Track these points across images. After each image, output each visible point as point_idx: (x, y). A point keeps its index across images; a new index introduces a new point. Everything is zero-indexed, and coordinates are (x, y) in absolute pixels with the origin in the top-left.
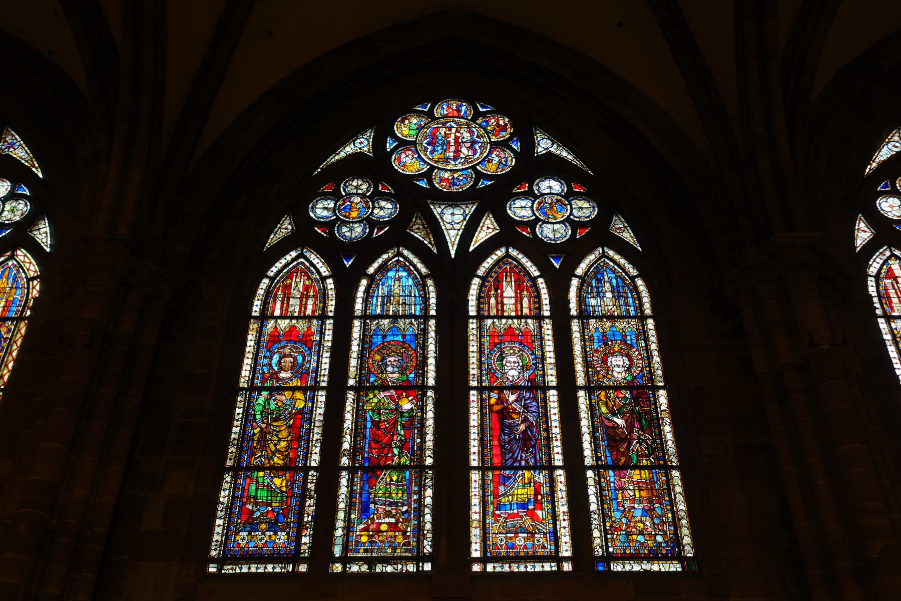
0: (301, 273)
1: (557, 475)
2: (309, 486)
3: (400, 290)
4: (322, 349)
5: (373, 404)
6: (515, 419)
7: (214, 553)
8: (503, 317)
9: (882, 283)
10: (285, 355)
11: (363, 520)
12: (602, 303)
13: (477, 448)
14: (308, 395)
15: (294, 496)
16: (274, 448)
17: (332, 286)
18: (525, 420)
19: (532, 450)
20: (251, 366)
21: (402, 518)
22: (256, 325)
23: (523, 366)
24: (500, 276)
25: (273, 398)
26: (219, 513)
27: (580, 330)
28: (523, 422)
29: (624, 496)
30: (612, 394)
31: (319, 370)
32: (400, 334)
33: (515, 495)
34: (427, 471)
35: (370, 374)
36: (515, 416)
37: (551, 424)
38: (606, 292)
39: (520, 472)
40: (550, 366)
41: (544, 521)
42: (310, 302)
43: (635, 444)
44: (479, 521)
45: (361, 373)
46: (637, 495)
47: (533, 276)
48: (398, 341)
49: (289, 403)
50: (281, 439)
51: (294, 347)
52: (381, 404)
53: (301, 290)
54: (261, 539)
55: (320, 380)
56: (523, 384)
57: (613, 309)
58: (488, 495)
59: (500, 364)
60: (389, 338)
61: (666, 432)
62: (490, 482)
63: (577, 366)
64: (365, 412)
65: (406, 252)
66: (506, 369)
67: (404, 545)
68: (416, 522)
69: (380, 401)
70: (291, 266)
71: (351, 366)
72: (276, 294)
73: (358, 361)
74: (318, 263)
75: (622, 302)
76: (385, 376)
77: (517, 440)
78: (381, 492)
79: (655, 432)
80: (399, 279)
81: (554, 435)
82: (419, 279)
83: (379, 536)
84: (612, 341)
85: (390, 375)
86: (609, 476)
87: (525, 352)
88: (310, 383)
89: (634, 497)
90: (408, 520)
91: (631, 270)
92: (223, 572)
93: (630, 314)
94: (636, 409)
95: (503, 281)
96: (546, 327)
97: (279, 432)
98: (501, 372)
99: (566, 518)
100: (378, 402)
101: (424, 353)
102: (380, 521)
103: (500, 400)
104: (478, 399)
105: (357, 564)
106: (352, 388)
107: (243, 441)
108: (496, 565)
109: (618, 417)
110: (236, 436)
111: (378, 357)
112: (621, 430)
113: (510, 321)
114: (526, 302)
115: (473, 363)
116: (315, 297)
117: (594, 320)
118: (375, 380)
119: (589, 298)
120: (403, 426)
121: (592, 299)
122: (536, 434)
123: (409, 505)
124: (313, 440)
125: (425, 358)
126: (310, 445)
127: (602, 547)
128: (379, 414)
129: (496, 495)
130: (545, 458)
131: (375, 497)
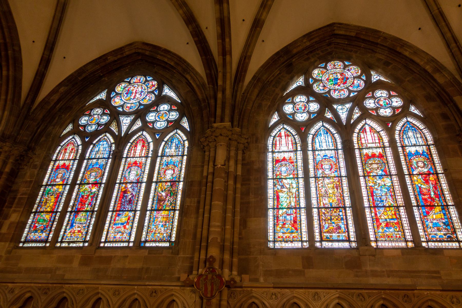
9: (275, 139)
17: (81, 148)
23: (136, 175)
28: (131, 195)
36: (128, 193)
39: (125, 212)
43: (166, 202)
48: (97, 167)
60: (95, 166)
75: (177, 150)
90: (85, 229)
91: (184, 138)
106: (78, 184)
111: (89, 173)
113: (137, 159)
114: (144, 151)
116: (74, 152)
120: (91, 197)
123: (86, 224)
125: (104, 173)
129: (115, 220)
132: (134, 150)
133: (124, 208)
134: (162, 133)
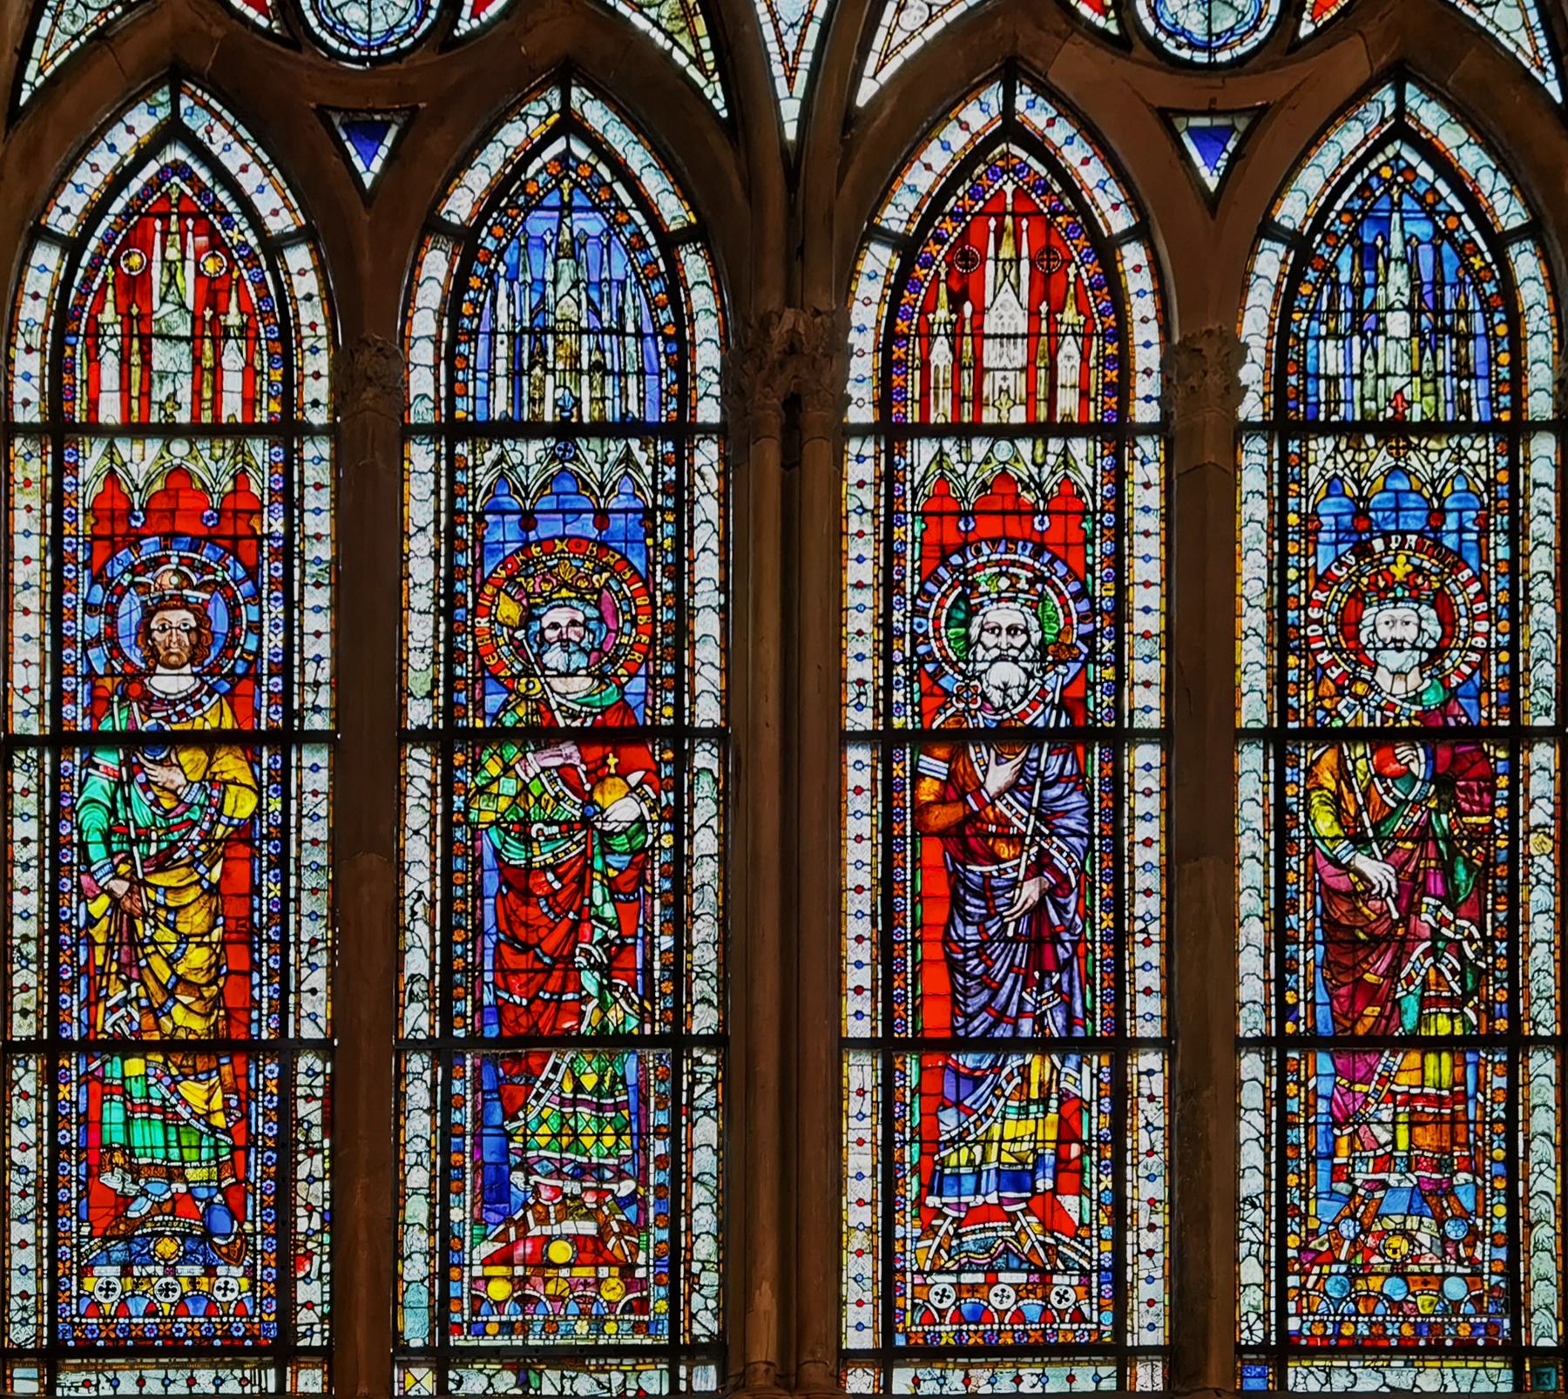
0: (182, 217)
1: (1139, 1073)
2: (303, 1109)
3: (579, 304)
4: (297, 572)
5: (503, 803)
6: (1005, 861)
7: (20, 1335)
8: (976, 429)
10: (162, 598)
11: (491, 1227)
12: (1369, 364)
13: (867, 970)
14: (265, 765)
15: (255, 1144)
16: (168, 973)
18: (1042, 864)
19: (1060, 981)
20: (42, 644)
21: (619, 1222)
22: (35, 464)
23: (1042, 646)
24: (974, 235)
25: (141, 778)
26: (15, 1201)
27: (1270, 488)
28: (1035, 870)
29: (1357, 1145)
30: (1361, 764)
31: (296, 661)
32: (584, 504)
33: (992, 1141)
34: (696, 1053)
35: (483, 678)
36: (1004, 850)
37: (1132, 880)
38: (1390, 308)
39: (1014, 1061)
40: (1143, 648)
41: (1082, 1233)
42: (233, 358)
43: (1418, 961)
44: (871, 1231)
45: (450, 678)
46: (1403, 1143)
47: (1106, 234)
48: (577, 541)
49: (201, 799)
50: (188, 936)
51: (191, 563)
52: (531, 800)
53: (190, 304)
54: (166, 1290)
55: (301, 705)
56: (1040, 723)
57: (1407, 391)
58: (904, 1142)
59: (958, 638)
61: (1533, 909)
62: (912, 1096)
63: (1246, 644)
64: (476, 834)
65: (596, 114)
66: (979, 658)
67: (630, 1307)
68: (664, 1235)
69: (525, 789)
70: (136, 185)
71: (411, 644)
72: (93, 318)
73: (437, 623)
74: (244, 169)
75: (1445, 359)
76: (538, 687)
77: (1008, 941)
78: (544, 1129)
79: (1494, 910)
80: (574, 249)
81: (1139, 925)
82: (655, 251)
83: (546, 1281)
84: (1386, 536)
85: (558, 684)
86: (1316, 1074)
87: (1053, 586)
88: (269, 717)
89: (1389, 1148)
90: (639, 1227)
92: (59, 1392)
93: (1469, 414)
94: (1438, 818)
95: (984, 259)
96: (1138, 473)
97: (176, 910)
98: (962, 672)
99: (1159, 1220)
100: (518, 794)
101: (678, 591)
102: (547, 1230)
103: (958, 787)
104: (874, 780)
105: (480, 1371)
106: (422, 736)
107: (56, 947)
108: (922, 1373)
109: (1372, 856)
110: (31, 928)
111: (509, 610)
112: (1378, 904)
113: (1003, 450)
115: (860, 633)
117: (1330, 443)
118: (504, 706)
119: (1318, 338)
120: (612, 887)
121: (1331, 343)
122: (1078, 920)
124: (298, 942)
125: (684, 613)
126: (292, 960)
127: (1264, 1317)
128: (527, 841)
129: (930, 1142)
130: (1103, 1009)
131: (525, 1149)
132: (955, 338)
133: (1000, 1017)
134: (1259, 115)
